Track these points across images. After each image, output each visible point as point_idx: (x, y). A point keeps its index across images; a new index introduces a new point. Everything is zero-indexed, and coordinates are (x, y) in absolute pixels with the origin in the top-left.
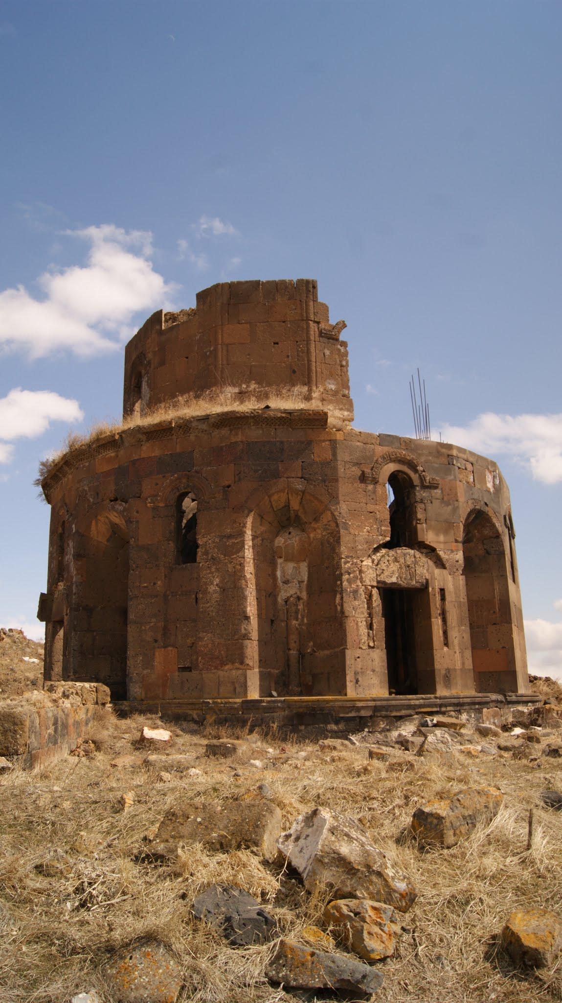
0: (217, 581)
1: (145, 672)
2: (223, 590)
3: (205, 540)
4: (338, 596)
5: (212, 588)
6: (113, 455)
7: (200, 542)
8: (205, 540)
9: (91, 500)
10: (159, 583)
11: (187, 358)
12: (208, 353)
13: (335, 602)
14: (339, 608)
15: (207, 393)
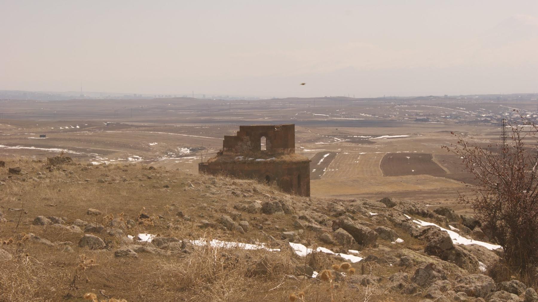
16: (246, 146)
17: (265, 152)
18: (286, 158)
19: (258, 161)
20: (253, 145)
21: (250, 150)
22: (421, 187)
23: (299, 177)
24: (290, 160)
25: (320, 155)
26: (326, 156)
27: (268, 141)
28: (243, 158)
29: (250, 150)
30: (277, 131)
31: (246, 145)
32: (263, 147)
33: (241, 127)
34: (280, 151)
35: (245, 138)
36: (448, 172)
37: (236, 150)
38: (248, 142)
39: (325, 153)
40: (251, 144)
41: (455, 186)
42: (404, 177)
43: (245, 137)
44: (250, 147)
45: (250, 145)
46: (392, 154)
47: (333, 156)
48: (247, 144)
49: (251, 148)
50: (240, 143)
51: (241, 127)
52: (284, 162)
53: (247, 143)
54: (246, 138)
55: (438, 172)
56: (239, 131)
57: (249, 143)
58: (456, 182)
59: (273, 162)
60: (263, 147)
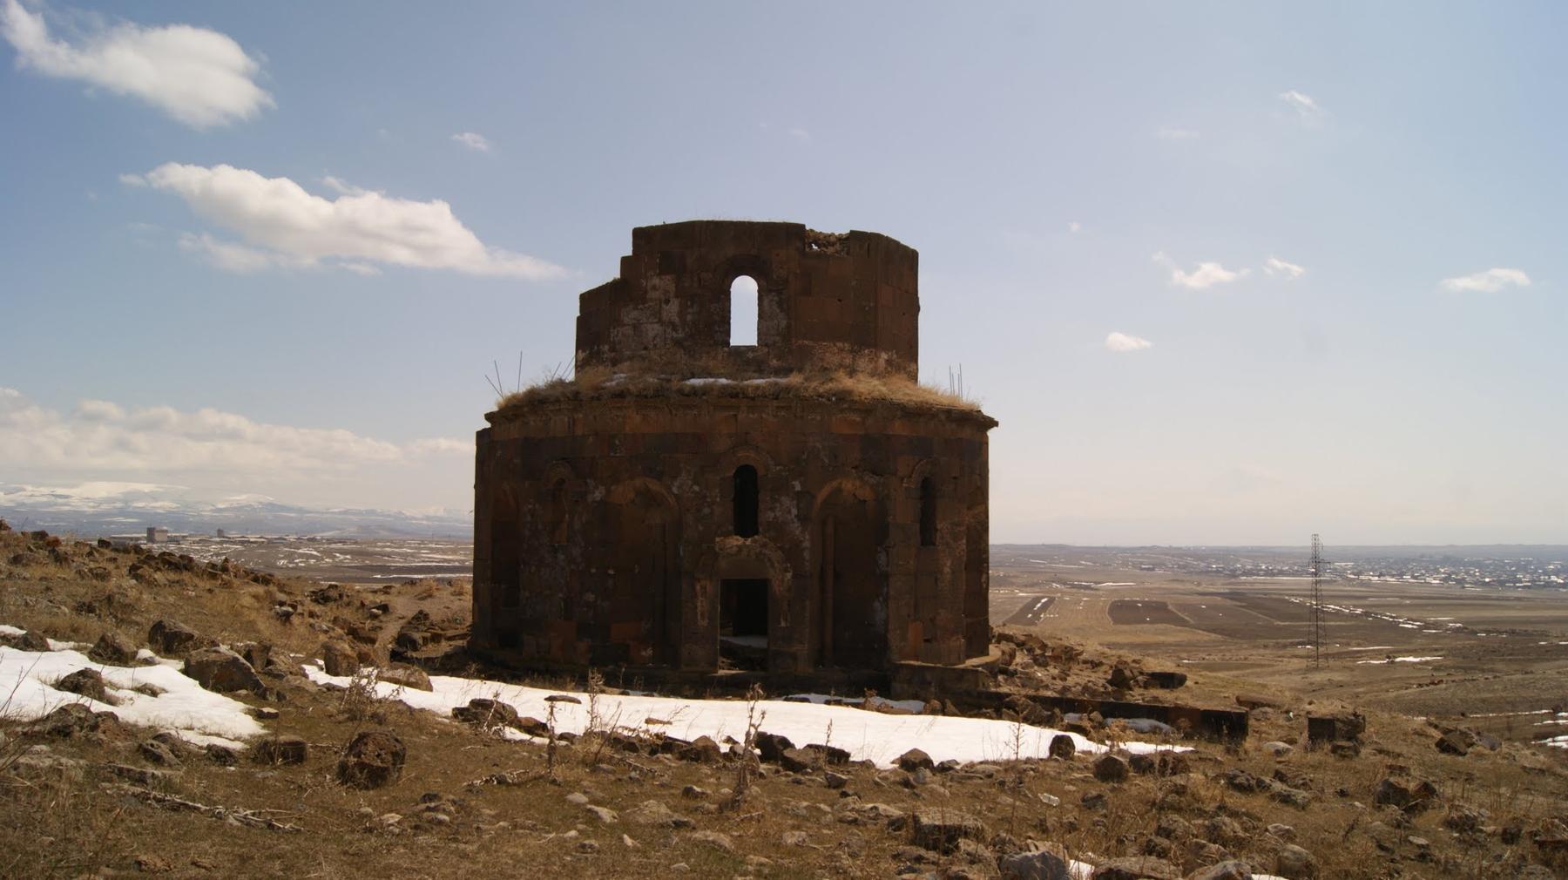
0: (949, 564)
1: (902, 644)
2: (953, 572)
3: (942, 525)
4: (984, 576)
5: (947, 570)
6: (858, 419)
7: (939, 527)
8: (942, 525)
9: (827, 461)
10: (911, 562)
11: (840, 300)
12: (867, 309)
13: (980, 581)
14: (985, 585)
15: (866, 351)
16: (656, 326)
17: (750, 355)
18: (866, 386)
19: (693, 387)
20: (689, 318)
21: (678, 343)
22: (1162, 638)
23: (928, 492)
24: (876, 394)
25: (1038, 600)
26: (1043, 601)
27: (766, 302)
28: (625, 378)
29: (678, 343)
30: (817, 255)
31: (660, 321)
32: (744, 329)
33: (640, 235)
34: (833, 354)
35: (654, 288)
36: (1192, 622)
37: (612, 349)
38: (667, 302)
39: (1043, 597)
40: (681, 314)
41: (1206, 638)
42: (1139, 627)
43: (656, 281)
44: (675, 329)
45: (677, 320)
46: (1120, 601)
47: (1051, 600)
48: (664, 317)
49: (681, 335)
50: (630, 315)
51: (640, 235)
52: (843, 397)
53: (660, 314)
54: (659, 284)
55: (1181, 622)
56: (629, 252)
57: (672, 310)
58: (1205, 633)
59: (777, 394)
60: (744, 329)
